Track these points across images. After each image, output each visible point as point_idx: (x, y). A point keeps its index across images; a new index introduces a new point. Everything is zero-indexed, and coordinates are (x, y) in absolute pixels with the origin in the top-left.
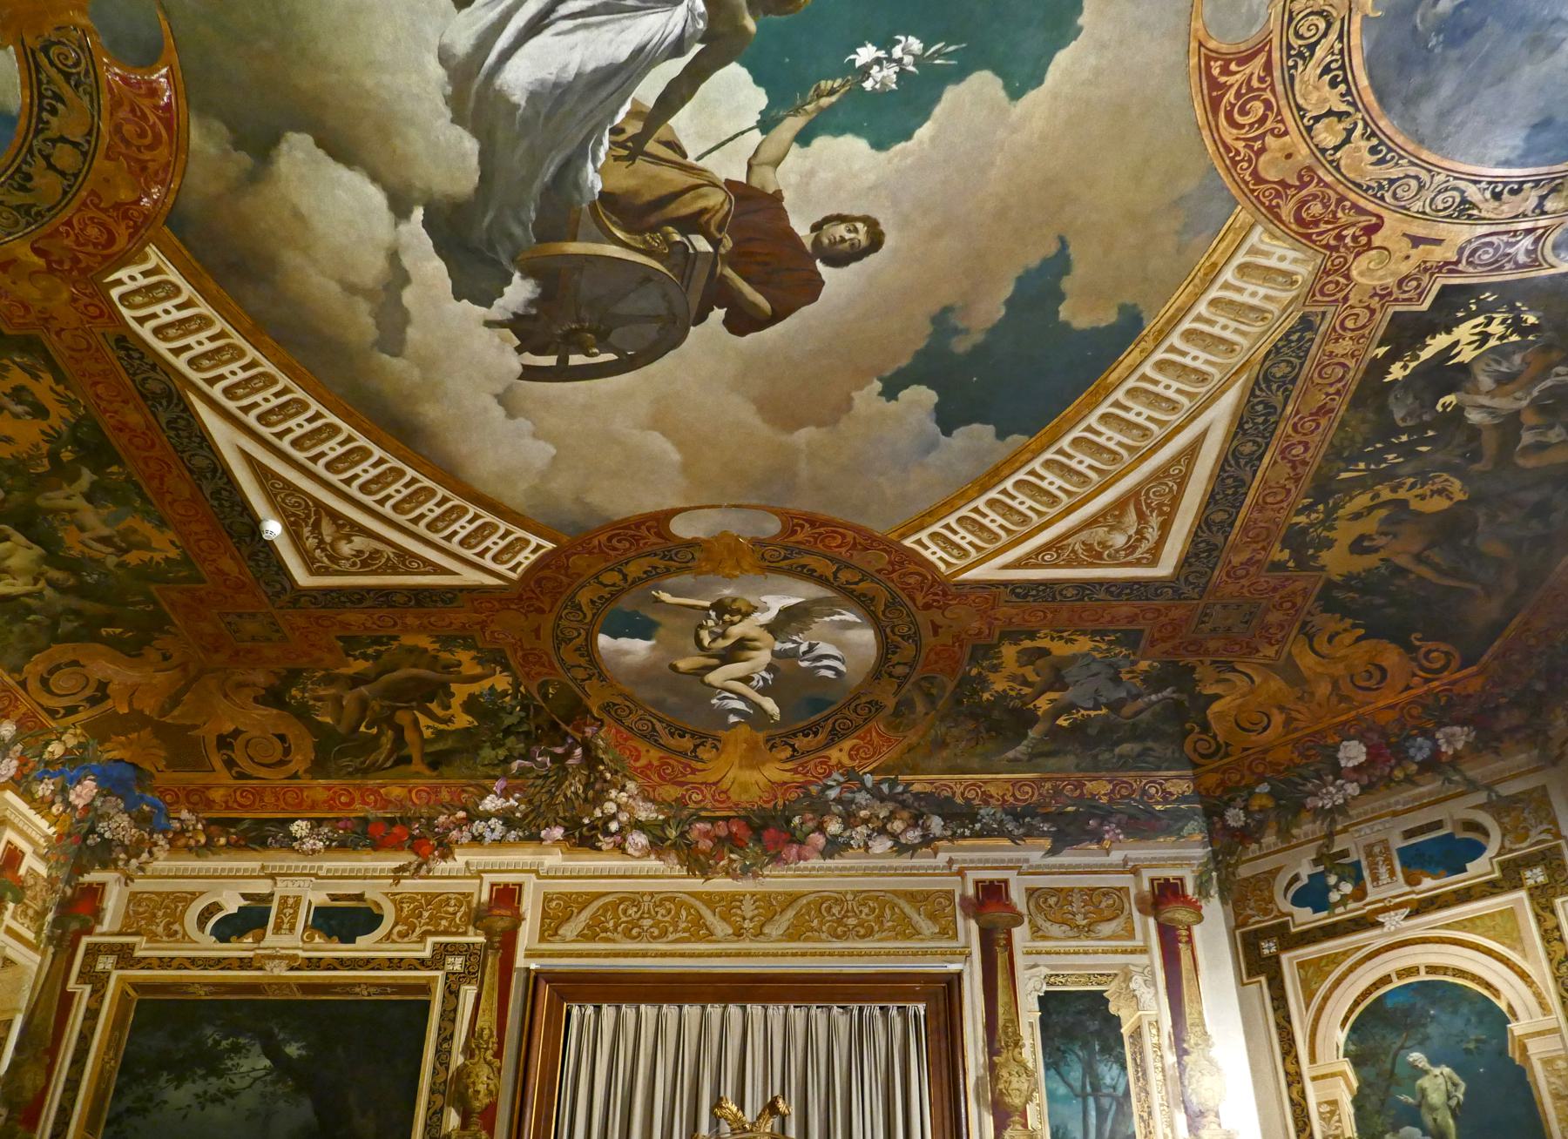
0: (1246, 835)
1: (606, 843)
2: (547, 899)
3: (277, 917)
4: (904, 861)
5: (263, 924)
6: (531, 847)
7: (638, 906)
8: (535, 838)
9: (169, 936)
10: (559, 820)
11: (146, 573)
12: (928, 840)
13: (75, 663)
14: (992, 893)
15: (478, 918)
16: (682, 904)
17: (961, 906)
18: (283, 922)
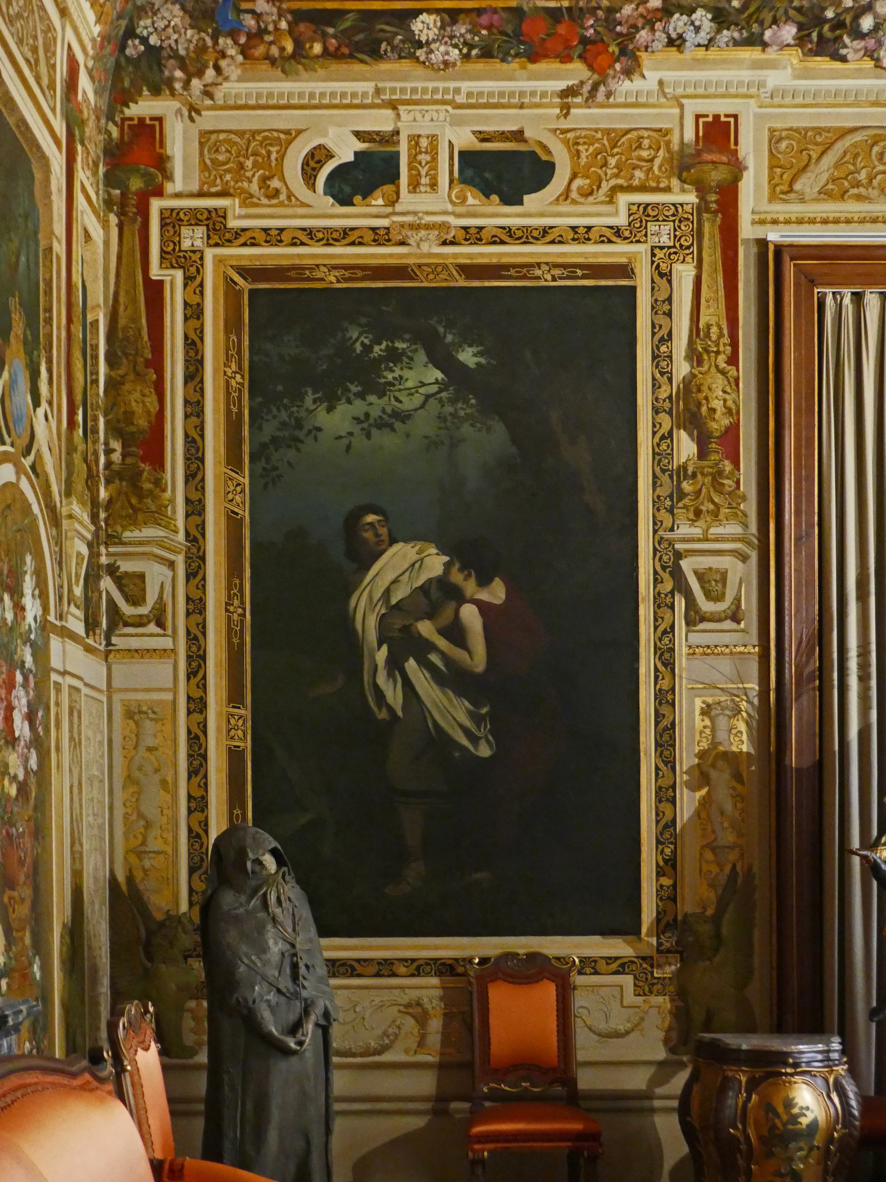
1: (851, 47)
3: (411, 168)
5: (394, 178)
6: (752, 54)
8: (755, 41)
9: (269, 197)
10: (792, 13)
18: (419, 175)
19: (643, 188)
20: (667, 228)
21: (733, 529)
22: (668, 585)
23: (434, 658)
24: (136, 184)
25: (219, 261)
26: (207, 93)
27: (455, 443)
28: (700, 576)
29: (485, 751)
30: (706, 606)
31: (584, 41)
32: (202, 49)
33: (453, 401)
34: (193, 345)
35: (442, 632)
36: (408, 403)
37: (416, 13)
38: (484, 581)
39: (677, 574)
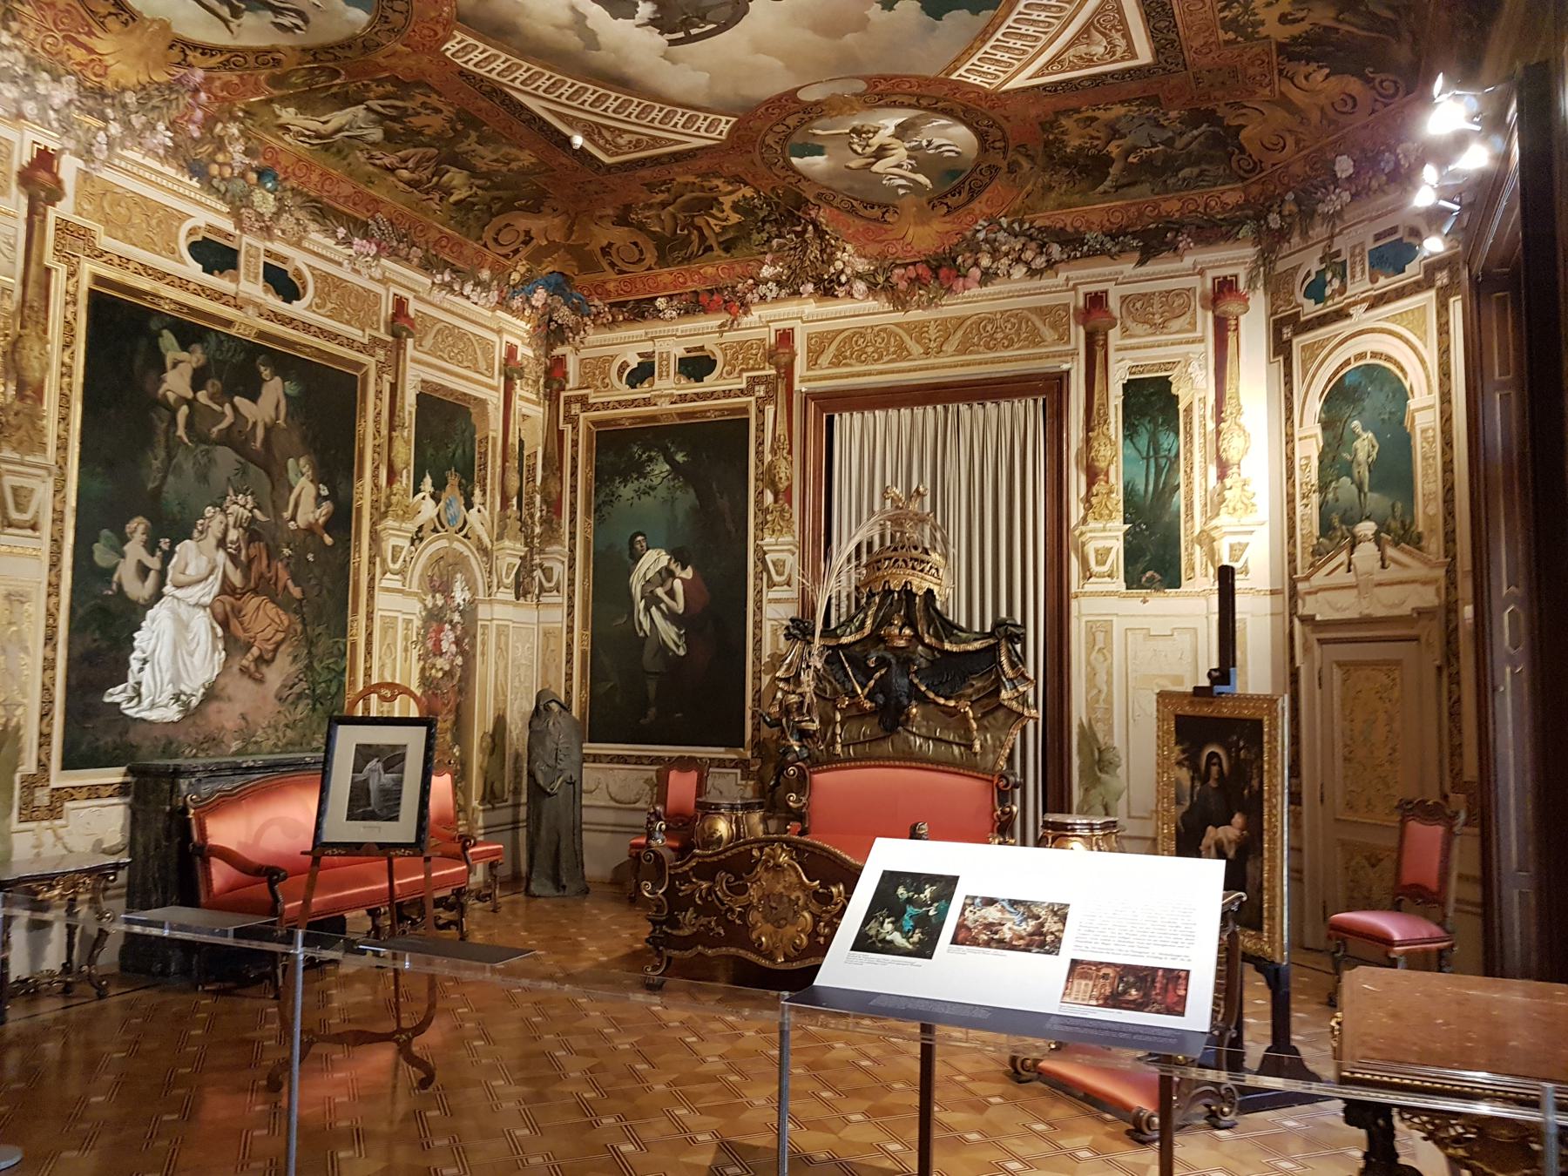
0: (1282, 235)
2: (809, 338)
4: (1036, 283)
7: (863, 336)
11: (523, 172)
12: (1051, 265)
13: (508, 225)
14: (1097, 301)
15: (771, 356)
16: (891, 334)
17: (1075, 315)
19: (753, 369)
20: (763, 387)
21: (788, 538)
22: (760, 567)
23: (663, 606)
24: (556, 386)
25: (585, 418)
26: (582, 342)
27: (674, 500)
28: (774, 564)
29: (682, 652)
30: (776, 578)
31: (725, 302)
32: (578, 323)
33: (673, 479)
34: (574, 459)
35: (666, 593)
36: (656, 481)
37: (656, 298)
38: (684, 568)
39: (764, 562)
